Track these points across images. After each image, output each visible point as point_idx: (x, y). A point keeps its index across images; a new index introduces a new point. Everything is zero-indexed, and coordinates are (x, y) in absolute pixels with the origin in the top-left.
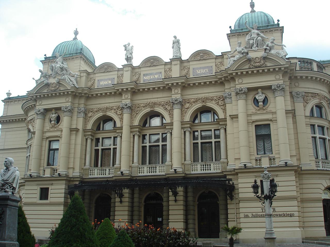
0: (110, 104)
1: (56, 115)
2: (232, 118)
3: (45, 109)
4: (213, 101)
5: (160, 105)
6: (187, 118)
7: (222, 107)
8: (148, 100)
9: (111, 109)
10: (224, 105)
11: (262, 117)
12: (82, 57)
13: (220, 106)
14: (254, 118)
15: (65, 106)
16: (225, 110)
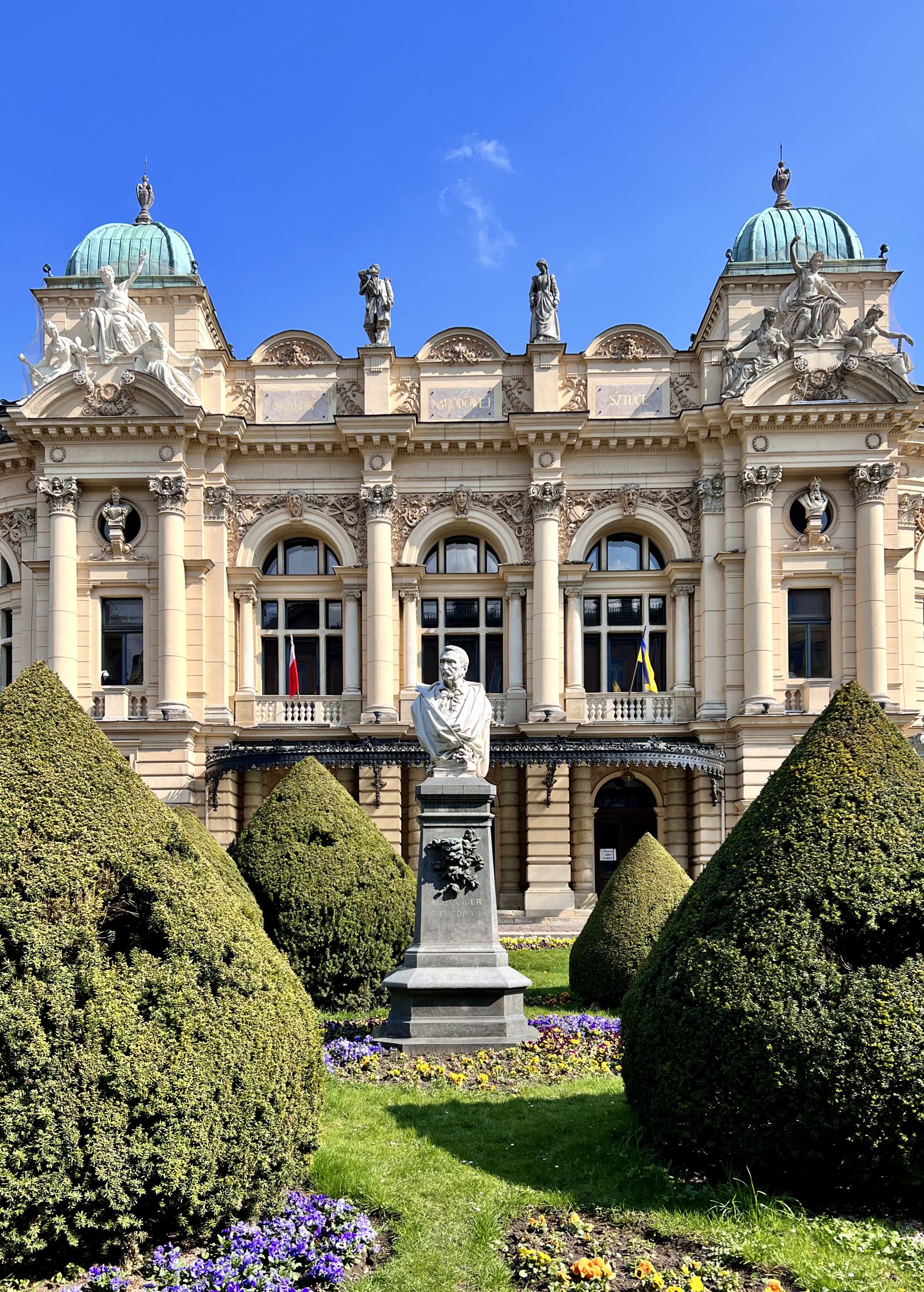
0: (317, 486)
1: (126, 510)
2: (720, 566)
3: (79, 483)
4: (659, 504)
5: (487, 504)
6: (578, 550)
7: (686, 525)
8: (449, 484)
9: (319, 502)
10: (696, 521)
11: (812, 566)
12: (203, 298)
13: (681, 521)
14: (790, 566)
15: (161, 477)
16: (695, 538)
